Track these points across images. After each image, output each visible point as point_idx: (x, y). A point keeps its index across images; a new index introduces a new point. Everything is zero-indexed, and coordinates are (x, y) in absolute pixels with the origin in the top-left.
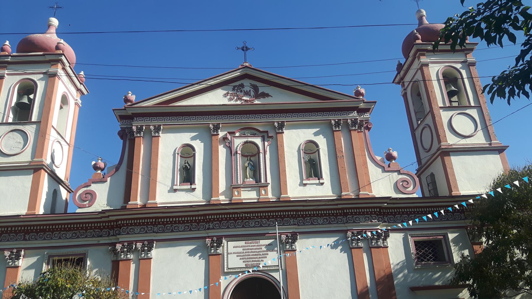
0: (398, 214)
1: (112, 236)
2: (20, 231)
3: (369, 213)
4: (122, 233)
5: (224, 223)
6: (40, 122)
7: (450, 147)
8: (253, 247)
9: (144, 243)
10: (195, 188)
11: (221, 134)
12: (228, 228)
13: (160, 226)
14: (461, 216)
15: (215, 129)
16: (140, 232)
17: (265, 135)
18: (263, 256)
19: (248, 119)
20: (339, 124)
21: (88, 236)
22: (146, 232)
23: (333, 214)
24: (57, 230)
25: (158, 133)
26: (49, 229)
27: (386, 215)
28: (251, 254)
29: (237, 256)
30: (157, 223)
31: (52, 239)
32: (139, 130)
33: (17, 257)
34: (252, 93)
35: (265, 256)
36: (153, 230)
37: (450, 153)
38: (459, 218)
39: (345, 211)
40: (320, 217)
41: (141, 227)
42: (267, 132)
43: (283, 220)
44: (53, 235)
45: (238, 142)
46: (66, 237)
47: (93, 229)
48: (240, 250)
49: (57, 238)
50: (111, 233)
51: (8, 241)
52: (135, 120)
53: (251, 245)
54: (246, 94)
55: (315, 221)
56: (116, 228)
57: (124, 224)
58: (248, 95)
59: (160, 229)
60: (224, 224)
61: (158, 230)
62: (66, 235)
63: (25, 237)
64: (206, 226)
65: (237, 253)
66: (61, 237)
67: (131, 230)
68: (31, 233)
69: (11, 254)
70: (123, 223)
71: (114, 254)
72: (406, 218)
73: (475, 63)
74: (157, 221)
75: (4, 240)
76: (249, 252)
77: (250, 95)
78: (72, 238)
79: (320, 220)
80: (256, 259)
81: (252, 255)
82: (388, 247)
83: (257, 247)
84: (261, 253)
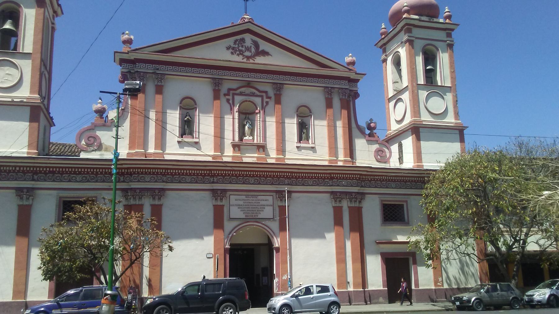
0: (373, 181)
2: (28, 172)
3: (351, 178)
5: (227, 178)
6: (31, 53)
7: (421, 123)
8: (252, 201)
11: (224, 90)
12: (230, 183)
14: (422, 186)
15: (217, 84)
16: (150, 180)
17: (264, 94)
18: (260, 209)
19: (249, 77)
20: (332, 93)
23: (321, 177)
24: (67, 173)
25: (161, 82)
26: (59, 171)
28: (250, 207)
29: (239, 208)
30: (166, 173)
31: (61, 181)
32: (142, 77)
33: (28, 197)
34: (253, 50)
35: (262, 209)
36: (163, 180)
37: (420, 128)
38: (420, 187)
39: (332, 176)
40: (311, 179)
41: (152, 176)
42: (266, 92)
43: (279, 180)
44: (63, 178)
46: (76, 180)
47: (103, 174)
48: (241, 203)
49: (67, 181)
50: (122, 179)
51: (16, 180)
52: (138, 66)
54: (247, 50)
55: (306, 182)
56: (126, 174)
57: (135, 172)
58: (249, 52)
59: (169, 179)
60: (227, 179)
61: (167, 180)
62: (76, 178)
63: (33, 177)
64: (210, 180)
65: (239, 205)
67: (142, 178)
69: (22, 193)
70: (134, 171)
71: (126, 199)
72: (379, 184)
73: (453, 44)
74: (167, 172)
75: (12, 179)
76: (248, 205)
77: (251, 52)
78: (83, 181)
79: (310, 182)
80: (255, 212)
81: (251, 208)
82: (362, 207)
83: (255, 201)
84: (259, 207)
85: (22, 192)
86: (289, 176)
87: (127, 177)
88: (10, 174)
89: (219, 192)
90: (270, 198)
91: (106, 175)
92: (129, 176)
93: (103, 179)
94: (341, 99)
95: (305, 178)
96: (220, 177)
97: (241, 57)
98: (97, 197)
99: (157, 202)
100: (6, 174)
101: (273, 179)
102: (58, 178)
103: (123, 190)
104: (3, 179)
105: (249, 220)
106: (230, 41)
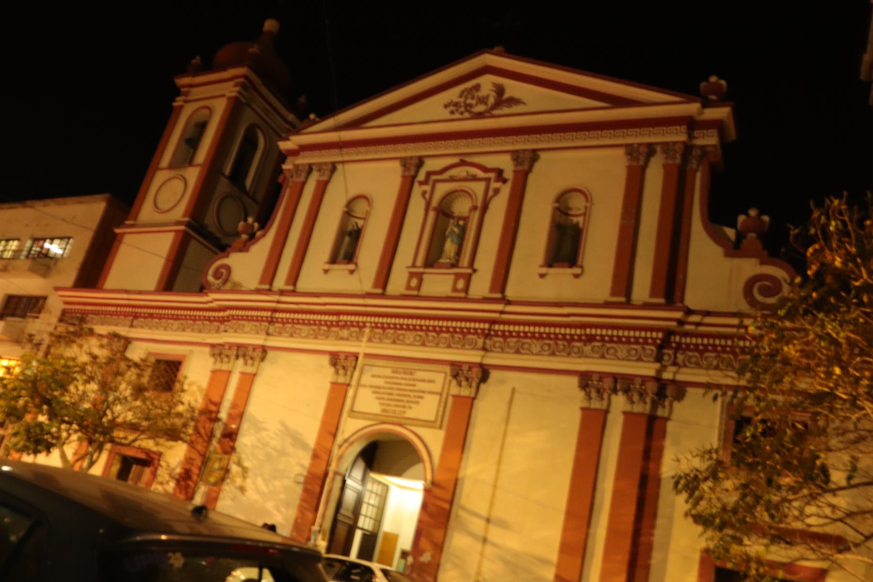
17: (492, 175)
18: (414, 399)
27: (682, 349)
28: (395, 392)
29: (374, 392)
34: (491, 101)
35: (417, 400)
40: (538, 339)
45: (442, 189)
48: (380, 382)
53: (398, 376)
65: (376, 387)
67: (241, 327)
76: (392, 389)
77: (486, 103)
80: (401, 404)
81: (399, 395)
84: (412, 394)
86: (486, 332)
89: (342, 357)
90: (439, 379)
94: (665, 166)
95: (526, 337)
96: (353, 329)
97: (467, 115)
99: (250, 370)
101: (453, 337)
103: (213, 346)
105: (385, 419)
106: (453, 94)
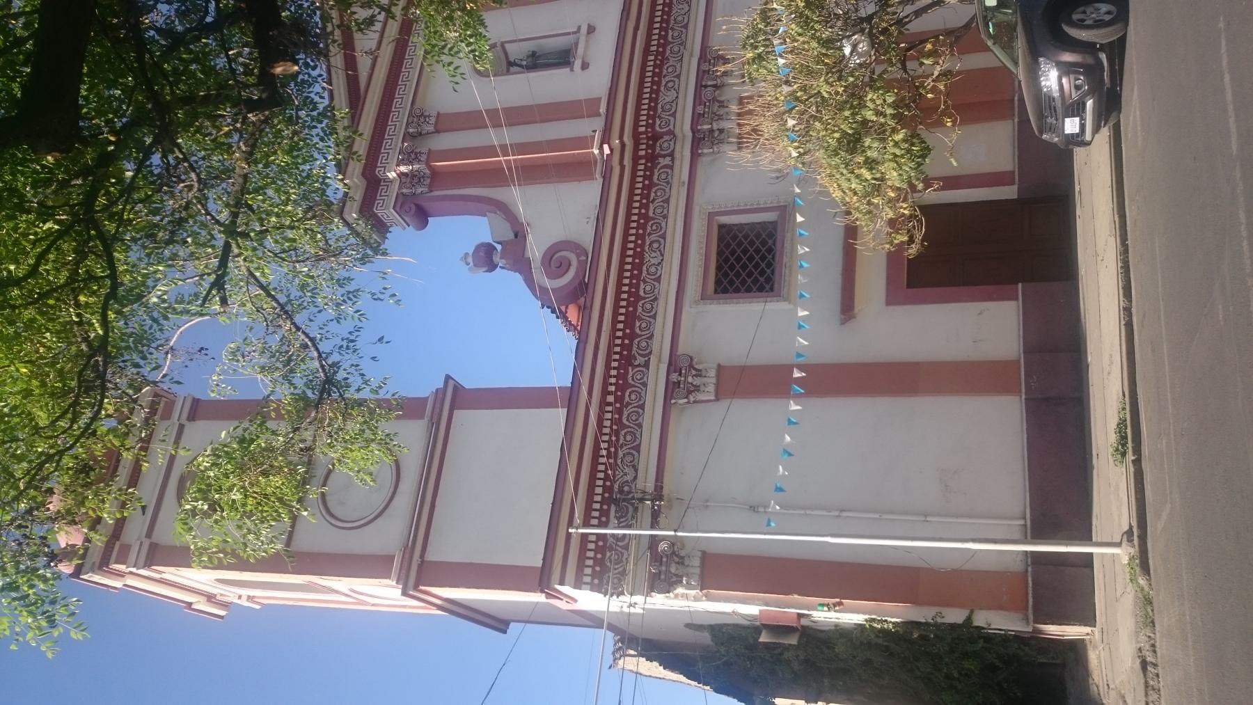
1: (673, 160)
4: (671, 127)
9: (704, 71)
10: (589, 26)
13: (668, 52)
21: (665, 212)
22: (678, 77)
24: (637, 286)
25: (429, 116)
33: (694, 372)
41: (662, 89)
46: (660, 263)
51: (642, 407)
56: (653, 147)
63: (639, 365)
66: (657, 276)
68: (631, 350)
69: (682, 386)
70: (644, 123)
85: (679, 387)
87: (661, 146)
88: (625, 421)
91: (652, 198)
92: (658, 144)
93: (662, 204)
98: (709, 213)
100: (623, 432)
102: (648, 306)
104: (636, 437)
